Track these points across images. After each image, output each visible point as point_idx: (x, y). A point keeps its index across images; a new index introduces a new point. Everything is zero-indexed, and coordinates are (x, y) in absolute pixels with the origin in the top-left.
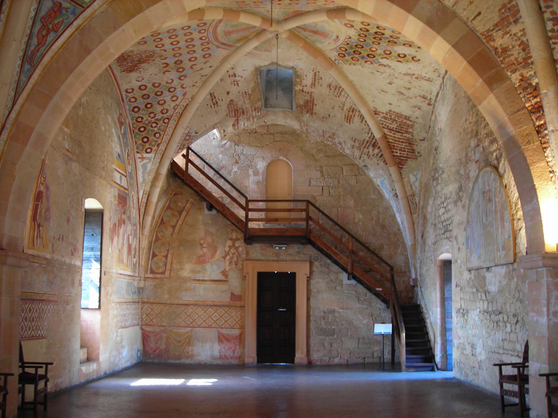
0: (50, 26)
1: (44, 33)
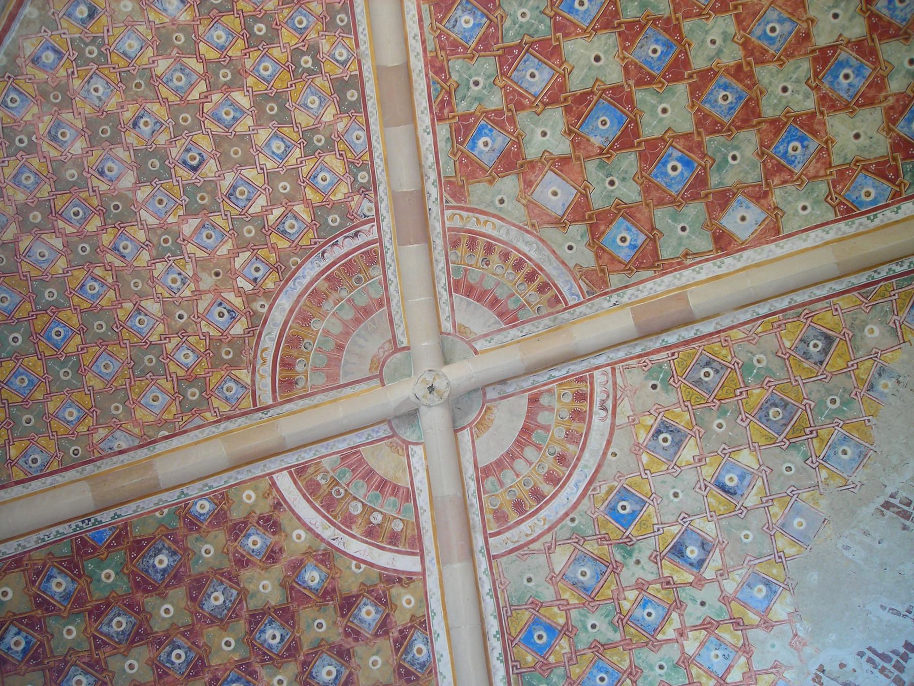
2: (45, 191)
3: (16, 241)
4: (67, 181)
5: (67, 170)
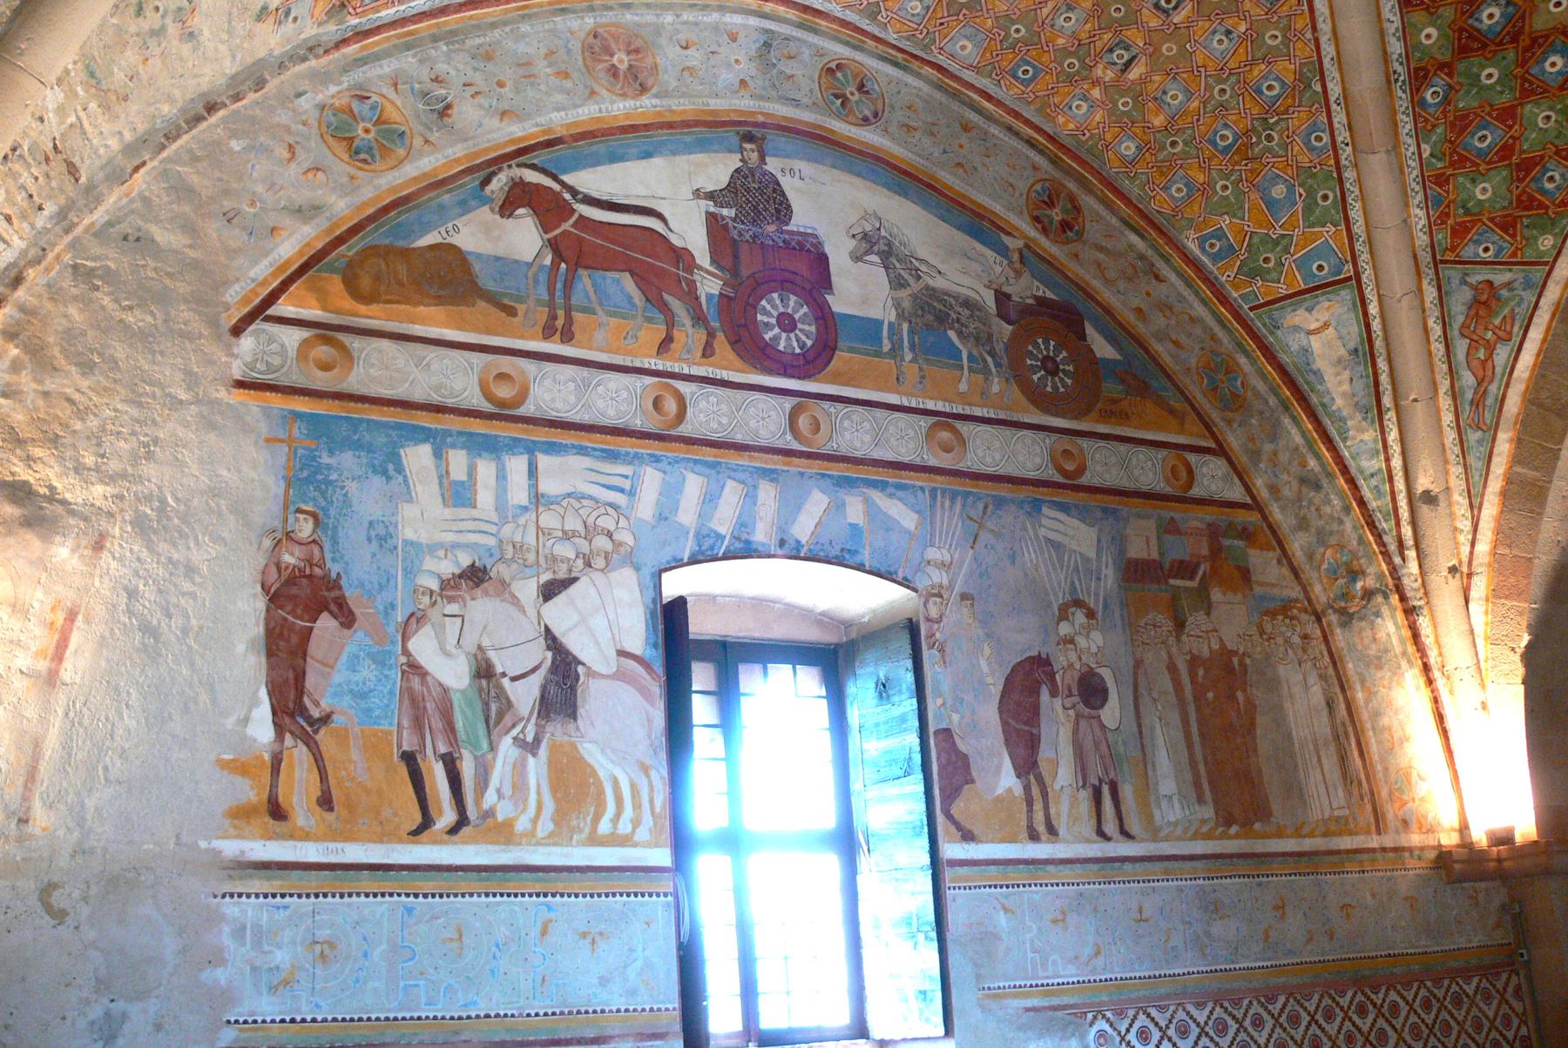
0: (1489, 335)
1: (1481, 354)
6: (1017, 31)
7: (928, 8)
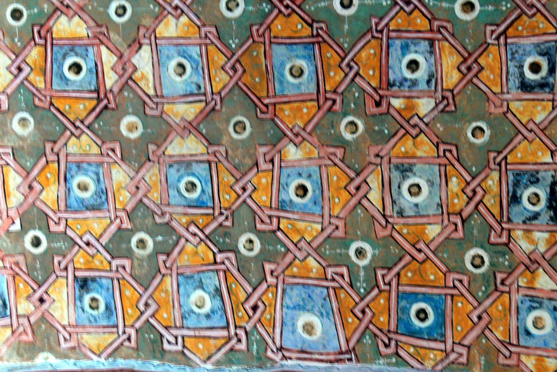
2: (82, 145)
3: (191, 127)
4: (38, 123)
5: (22, 138)
6: (360, 253)
7: (218, 291)
